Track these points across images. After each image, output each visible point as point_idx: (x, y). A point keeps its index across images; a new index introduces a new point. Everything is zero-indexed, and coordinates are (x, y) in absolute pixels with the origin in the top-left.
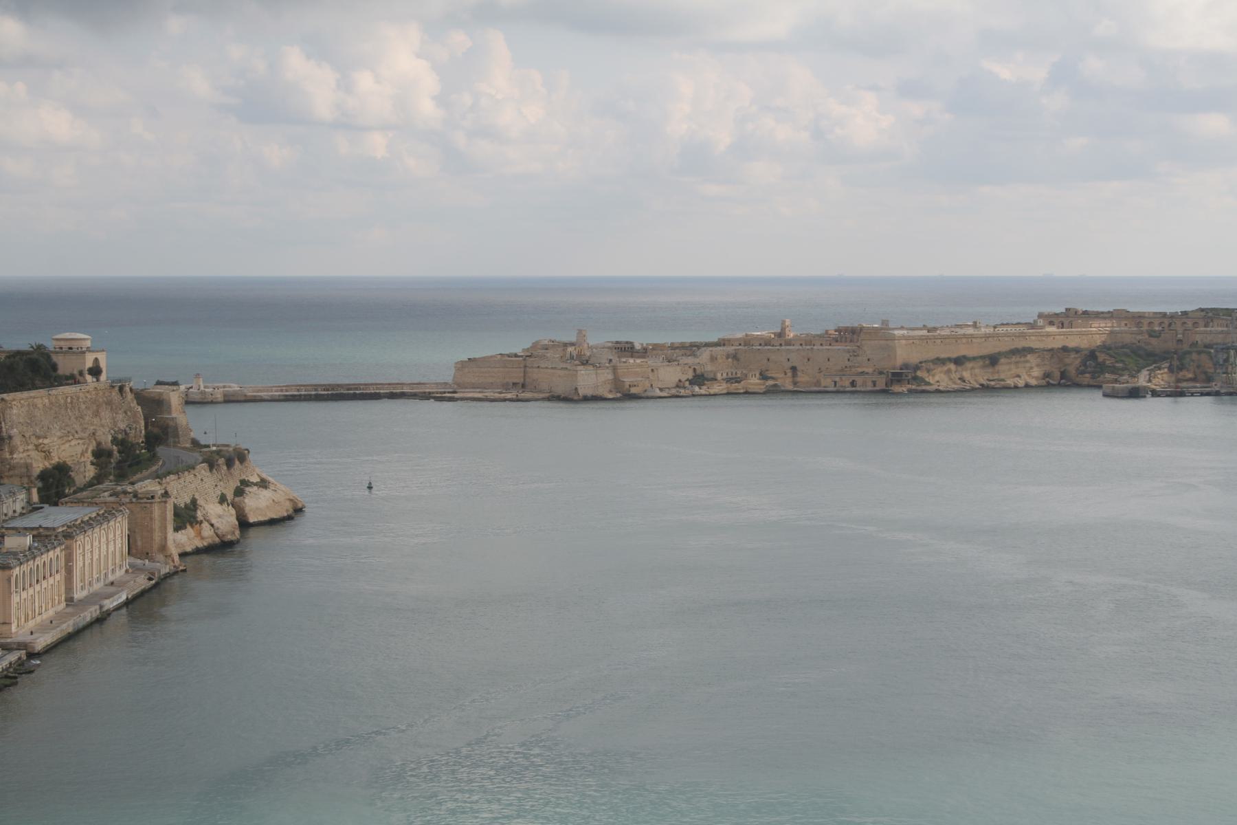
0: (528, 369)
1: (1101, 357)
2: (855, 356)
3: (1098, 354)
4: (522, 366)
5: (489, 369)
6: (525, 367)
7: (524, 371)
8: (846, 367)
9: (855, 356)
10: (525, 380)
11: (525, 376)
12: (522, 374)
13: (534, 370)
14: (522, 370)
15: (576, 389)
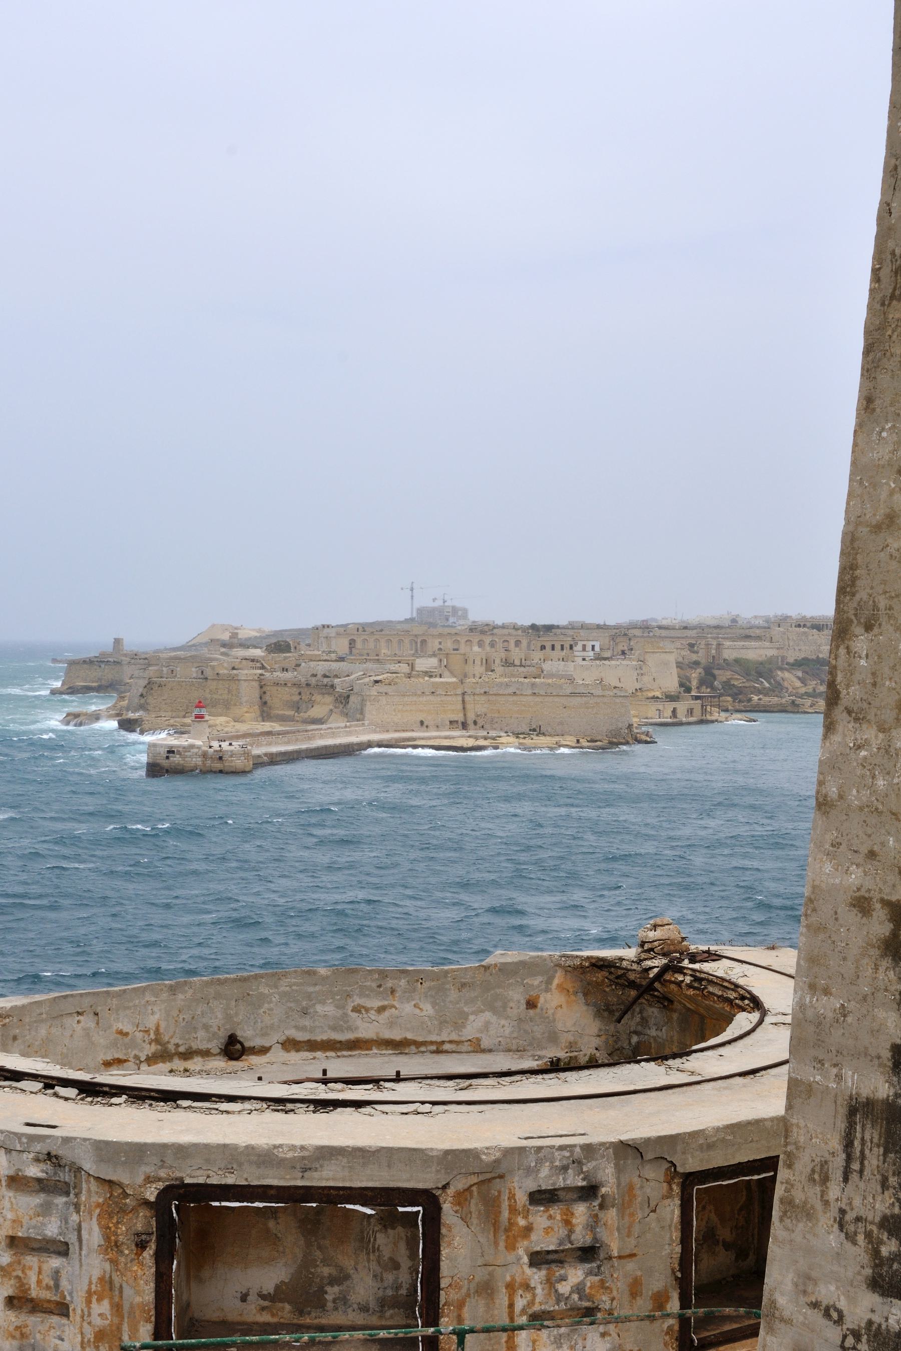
0: (467, 698)
1: (722, 676)
2: (642, 674)
3: (716, 672)
4: (459, 691)
5: (415, 698)
6: (464, 694)
7: (463, 701)
8: (636, 690)
9: (642, 674)
10: (465, 715)
11: (464, 708)
12: (460, 707)
13: (476, 697)
14: (460, 698)
15: (630, 726)
